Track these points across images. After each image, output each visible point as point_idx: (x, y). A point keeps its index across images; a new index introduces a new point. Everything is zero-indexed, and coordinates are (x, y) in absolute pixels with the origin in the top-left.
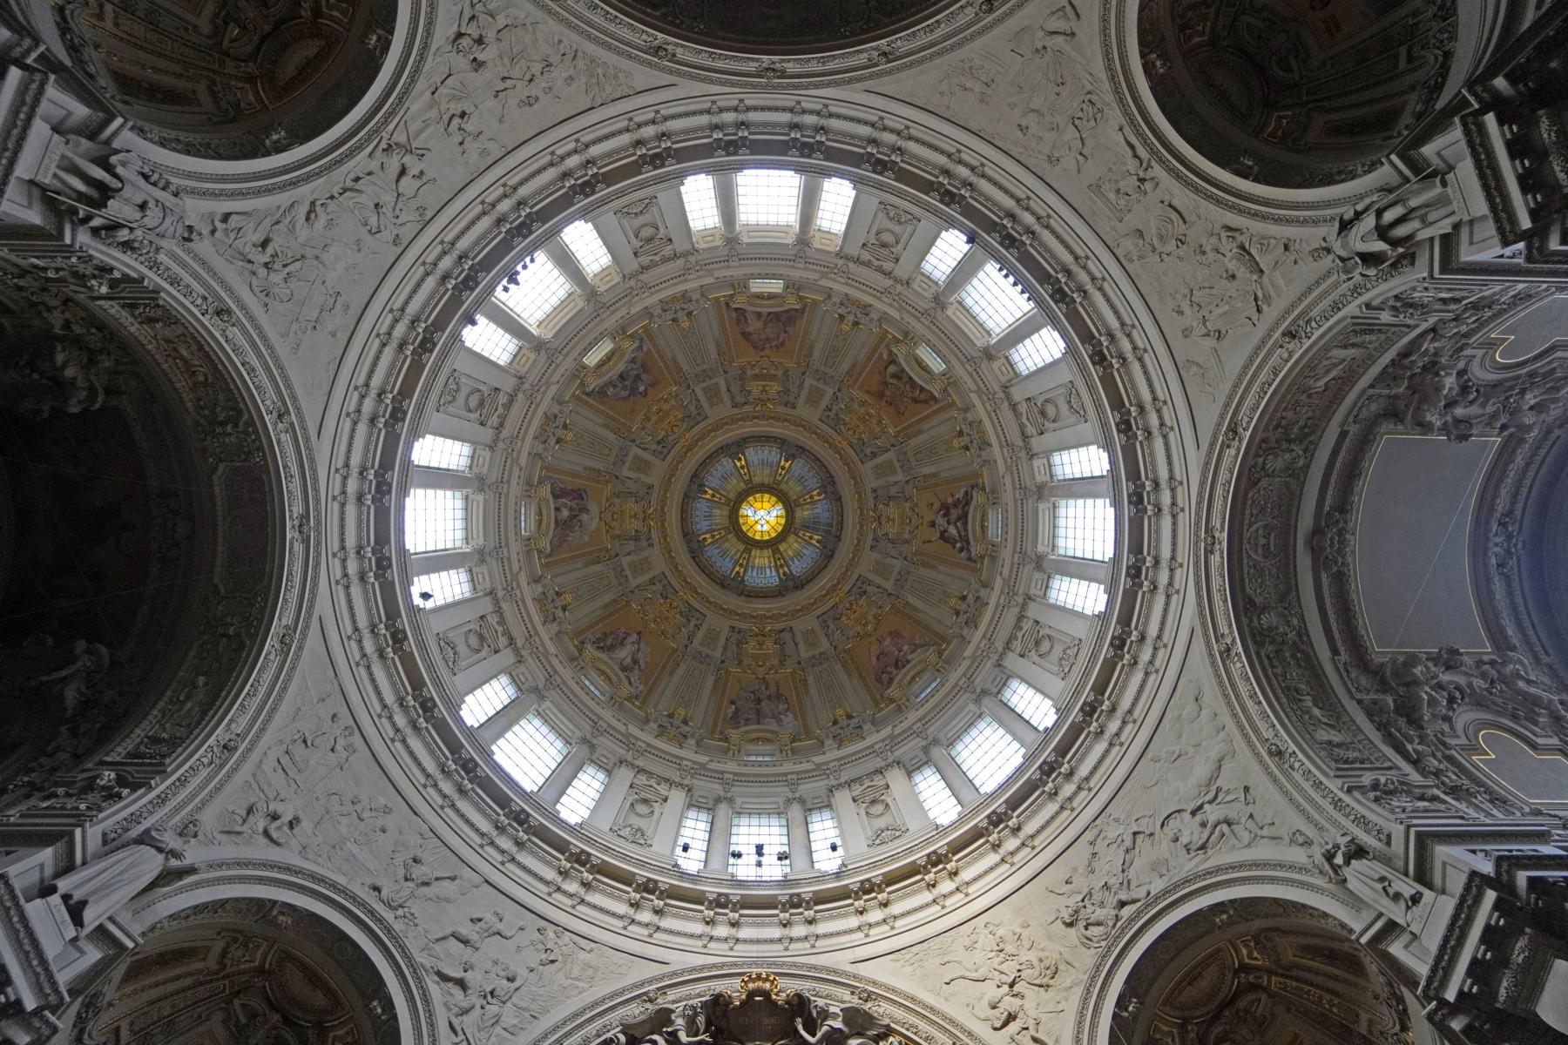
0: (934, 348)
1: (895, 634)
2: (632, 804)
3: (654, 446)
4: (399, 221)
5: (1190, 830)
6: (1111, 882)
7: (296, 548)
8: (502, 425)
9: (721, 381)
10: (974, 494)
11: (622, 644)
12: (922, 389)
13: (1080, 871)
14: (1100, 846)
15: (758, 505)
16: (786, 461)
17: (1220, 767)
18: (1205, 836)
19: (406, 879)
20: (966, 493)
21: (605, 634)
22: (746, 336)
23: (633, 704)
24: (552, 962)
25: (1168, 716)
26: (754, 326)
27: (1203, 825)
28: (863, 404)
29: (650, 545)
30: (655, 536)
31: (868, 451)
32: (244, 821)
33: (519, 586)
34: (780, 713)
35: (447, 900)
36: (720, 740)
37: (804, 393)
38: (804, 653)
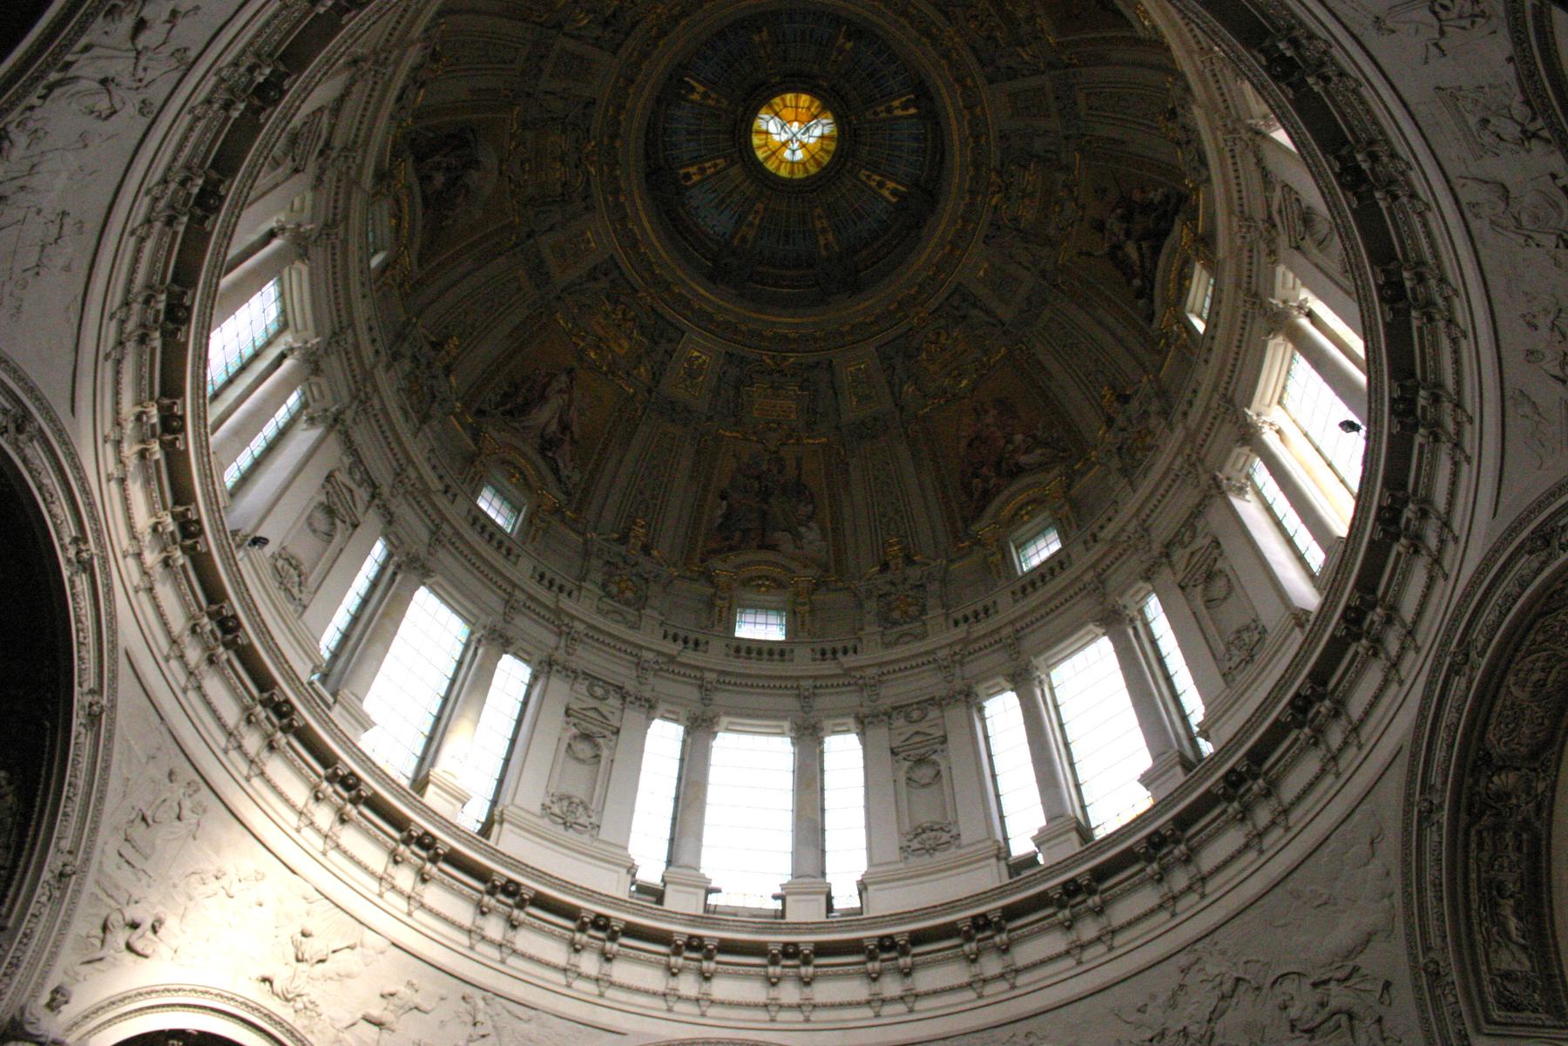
2: (569, 745)
4: (144, 83)
5: (1303, 1003)
6: (1193, 1028)
7: (78, 582)
10: (1178, 222)
11: (543, 398)
13: (1160, 1001)
14: (1193, 979)
15: (788, 113)
17: (1368, 941)
18: (1318, 1019)
19: (298, 960)
20: (1167, 197)
24: (483, 1036)
25: (1332, 844)
27: (1323, 1005)
32: (103, 942)
35: (349, 976)
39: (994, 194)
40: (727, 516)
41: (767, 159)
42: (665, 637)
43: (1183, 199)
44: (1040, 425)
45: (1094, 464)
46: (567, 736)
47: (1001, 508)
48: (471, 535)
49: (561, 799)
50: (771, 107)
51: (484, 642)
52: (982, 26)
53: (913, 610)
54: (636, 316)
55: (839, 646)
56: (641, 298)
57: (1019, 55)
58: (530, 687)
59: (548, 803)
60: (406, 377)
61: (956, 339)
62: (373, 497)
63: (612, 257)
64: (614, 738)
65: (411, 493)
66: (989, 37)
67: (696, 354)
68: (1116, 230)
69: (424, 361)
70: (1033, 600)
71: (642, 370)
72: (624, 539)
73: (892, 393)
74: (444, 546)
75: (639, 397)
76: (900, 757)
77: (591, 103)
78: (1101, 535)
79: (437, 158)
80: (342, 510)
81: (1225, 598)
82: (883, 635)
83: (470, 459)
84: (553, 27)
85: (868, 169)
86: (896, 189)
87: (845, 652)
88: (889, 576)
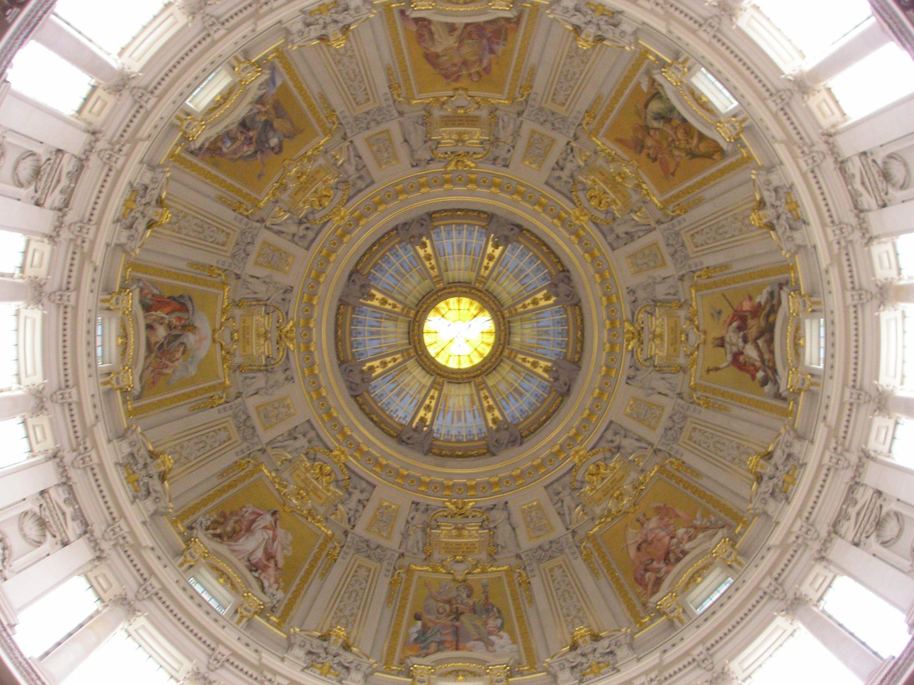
0: (718, 75)
1: (663, 511)
3: (293, 229)
8: (67, 203)
9: (394, 127)
10: (784, 295)
11: (249, 530)
12: (702, 137)
16: (496, 246)
20: (772, 294)
21: (223, 515)
22: (432, 59)
23: (268, 620)
26: (444, 43)
28: (612, 159)
29: (290, 379)
33: (95, 445)
36: (399, 673)
37: (521, 144)
38: (527, 543)
39: (628, 341)
50: (438, 311)
52: (600, 203)
54: (332, 471)
56: (336, 456)
57: (633, 219)
63: (309, 421)
66: (607, 212)
68: (734, 340)
69: (141, 461)
73: (564, 521)
79: (160, 314)
80: (55, 528)
81: (898, 536)
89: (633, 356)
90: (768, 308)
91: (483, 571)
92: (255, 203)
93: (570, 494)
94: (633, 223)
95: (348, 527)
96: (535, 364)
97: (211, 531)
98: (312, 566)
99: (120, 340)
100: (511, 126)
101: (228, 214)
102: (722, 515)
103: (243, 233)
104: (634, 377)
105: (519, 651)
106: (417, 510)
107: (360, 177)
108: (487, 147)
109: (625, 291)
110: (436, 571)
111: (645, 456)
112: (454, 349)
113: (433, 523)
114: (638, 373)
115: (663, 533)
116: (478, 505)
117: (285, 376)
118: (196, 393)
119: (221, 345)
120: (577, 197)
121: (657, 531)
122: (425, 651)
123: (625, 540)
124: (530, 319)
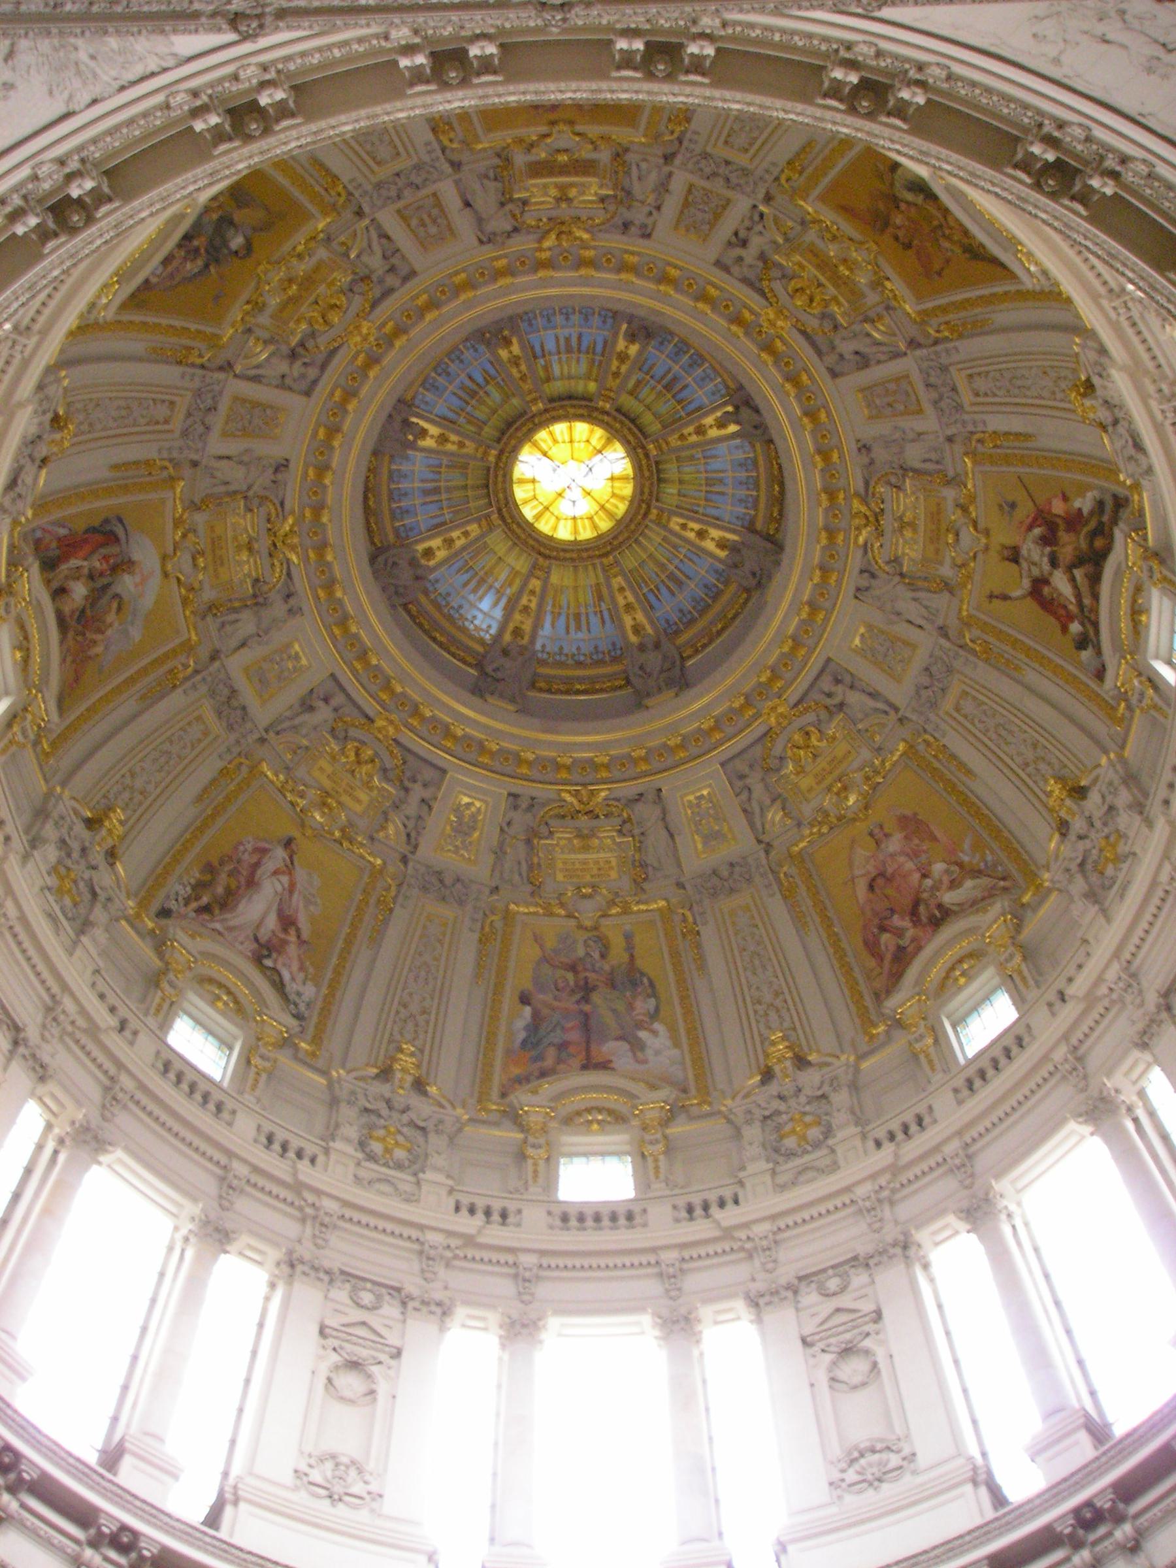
1: (912, 825)
2: (329, 1380)
3: (283, 367)
10: (1118, 534)
11: (252, 883)
20: (1101, 504)
30: (301, 584)
31: (847, 348)
34: (639, 1026)
37: (672, 205)
39: (858, 529)
40: (534, 1026)
41: (538, 517)
42: (457, 1209)
43: (1120, 503)
44: (966, 846)
45: (1049, 891)
46: (324, 1370)
47: (925, 971)
48: (164, 1088)
49: (321, 1461)
51: (193, 1239)
52: (811, 300)
53: (814, 1133)
54: (376, 754)
55: (712, 1197)
56: (380, 730)
57: (868, 335)
58: (267, 1299)
59: (303, 1467)
60: (53, 870)
61: (834, 738)
62: (16, 1043)
63: (332, 675)
64: (393, 1363)
65: (71, 1035)
66: (823, 316)
67: (466, 800)
68: (1036, 557)
69: (75, 846)
70: (987, 1094)
71: (391, 830)
72: (385, 1074)
73: (752, 825)
74: (125, 1107)
75: (391, 869)
76: (816, 1349)
77: (282, 466)
78: (1070, 991)
79: (74, 562)
82: (774, 1173)
83: (154, 980)
84: (221, 369)
85: (681, 516)
86: (722, 539)
87: (722, 1204)
88: (773, 1088)
89: (866, 552)
90: (1093, 524)
91: (626, 911)
92: (213, 341)
93: (763, 779)
94: (868, 341)
95: (404, 849)
96: (701, 534)
97: (194, 905)
98: (354, 927)
99: (18, 655)
100: (654, 176)
101: (168, 374)
102: (1002, 855)
103: (198, 394)
104: (867, 589)
105: (683, 1063)
106: (516, 808)
107: (392, 269)
108: (612, 208)
109: (854, 446)
110: (551, 914)
111: (883, 725)
112: (564, 508)
113: (544, 830)
114: (874, 582)
115: (910, 865)
116: (617, 794)
117: (286, 607)
118: (144, 671)
119: (178, 580)
120: (772, 290)
121: (902, 859)
122: (539, 1064)
123: (851, 865)
124: (692, 458)
